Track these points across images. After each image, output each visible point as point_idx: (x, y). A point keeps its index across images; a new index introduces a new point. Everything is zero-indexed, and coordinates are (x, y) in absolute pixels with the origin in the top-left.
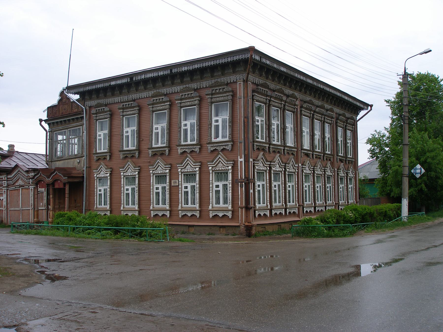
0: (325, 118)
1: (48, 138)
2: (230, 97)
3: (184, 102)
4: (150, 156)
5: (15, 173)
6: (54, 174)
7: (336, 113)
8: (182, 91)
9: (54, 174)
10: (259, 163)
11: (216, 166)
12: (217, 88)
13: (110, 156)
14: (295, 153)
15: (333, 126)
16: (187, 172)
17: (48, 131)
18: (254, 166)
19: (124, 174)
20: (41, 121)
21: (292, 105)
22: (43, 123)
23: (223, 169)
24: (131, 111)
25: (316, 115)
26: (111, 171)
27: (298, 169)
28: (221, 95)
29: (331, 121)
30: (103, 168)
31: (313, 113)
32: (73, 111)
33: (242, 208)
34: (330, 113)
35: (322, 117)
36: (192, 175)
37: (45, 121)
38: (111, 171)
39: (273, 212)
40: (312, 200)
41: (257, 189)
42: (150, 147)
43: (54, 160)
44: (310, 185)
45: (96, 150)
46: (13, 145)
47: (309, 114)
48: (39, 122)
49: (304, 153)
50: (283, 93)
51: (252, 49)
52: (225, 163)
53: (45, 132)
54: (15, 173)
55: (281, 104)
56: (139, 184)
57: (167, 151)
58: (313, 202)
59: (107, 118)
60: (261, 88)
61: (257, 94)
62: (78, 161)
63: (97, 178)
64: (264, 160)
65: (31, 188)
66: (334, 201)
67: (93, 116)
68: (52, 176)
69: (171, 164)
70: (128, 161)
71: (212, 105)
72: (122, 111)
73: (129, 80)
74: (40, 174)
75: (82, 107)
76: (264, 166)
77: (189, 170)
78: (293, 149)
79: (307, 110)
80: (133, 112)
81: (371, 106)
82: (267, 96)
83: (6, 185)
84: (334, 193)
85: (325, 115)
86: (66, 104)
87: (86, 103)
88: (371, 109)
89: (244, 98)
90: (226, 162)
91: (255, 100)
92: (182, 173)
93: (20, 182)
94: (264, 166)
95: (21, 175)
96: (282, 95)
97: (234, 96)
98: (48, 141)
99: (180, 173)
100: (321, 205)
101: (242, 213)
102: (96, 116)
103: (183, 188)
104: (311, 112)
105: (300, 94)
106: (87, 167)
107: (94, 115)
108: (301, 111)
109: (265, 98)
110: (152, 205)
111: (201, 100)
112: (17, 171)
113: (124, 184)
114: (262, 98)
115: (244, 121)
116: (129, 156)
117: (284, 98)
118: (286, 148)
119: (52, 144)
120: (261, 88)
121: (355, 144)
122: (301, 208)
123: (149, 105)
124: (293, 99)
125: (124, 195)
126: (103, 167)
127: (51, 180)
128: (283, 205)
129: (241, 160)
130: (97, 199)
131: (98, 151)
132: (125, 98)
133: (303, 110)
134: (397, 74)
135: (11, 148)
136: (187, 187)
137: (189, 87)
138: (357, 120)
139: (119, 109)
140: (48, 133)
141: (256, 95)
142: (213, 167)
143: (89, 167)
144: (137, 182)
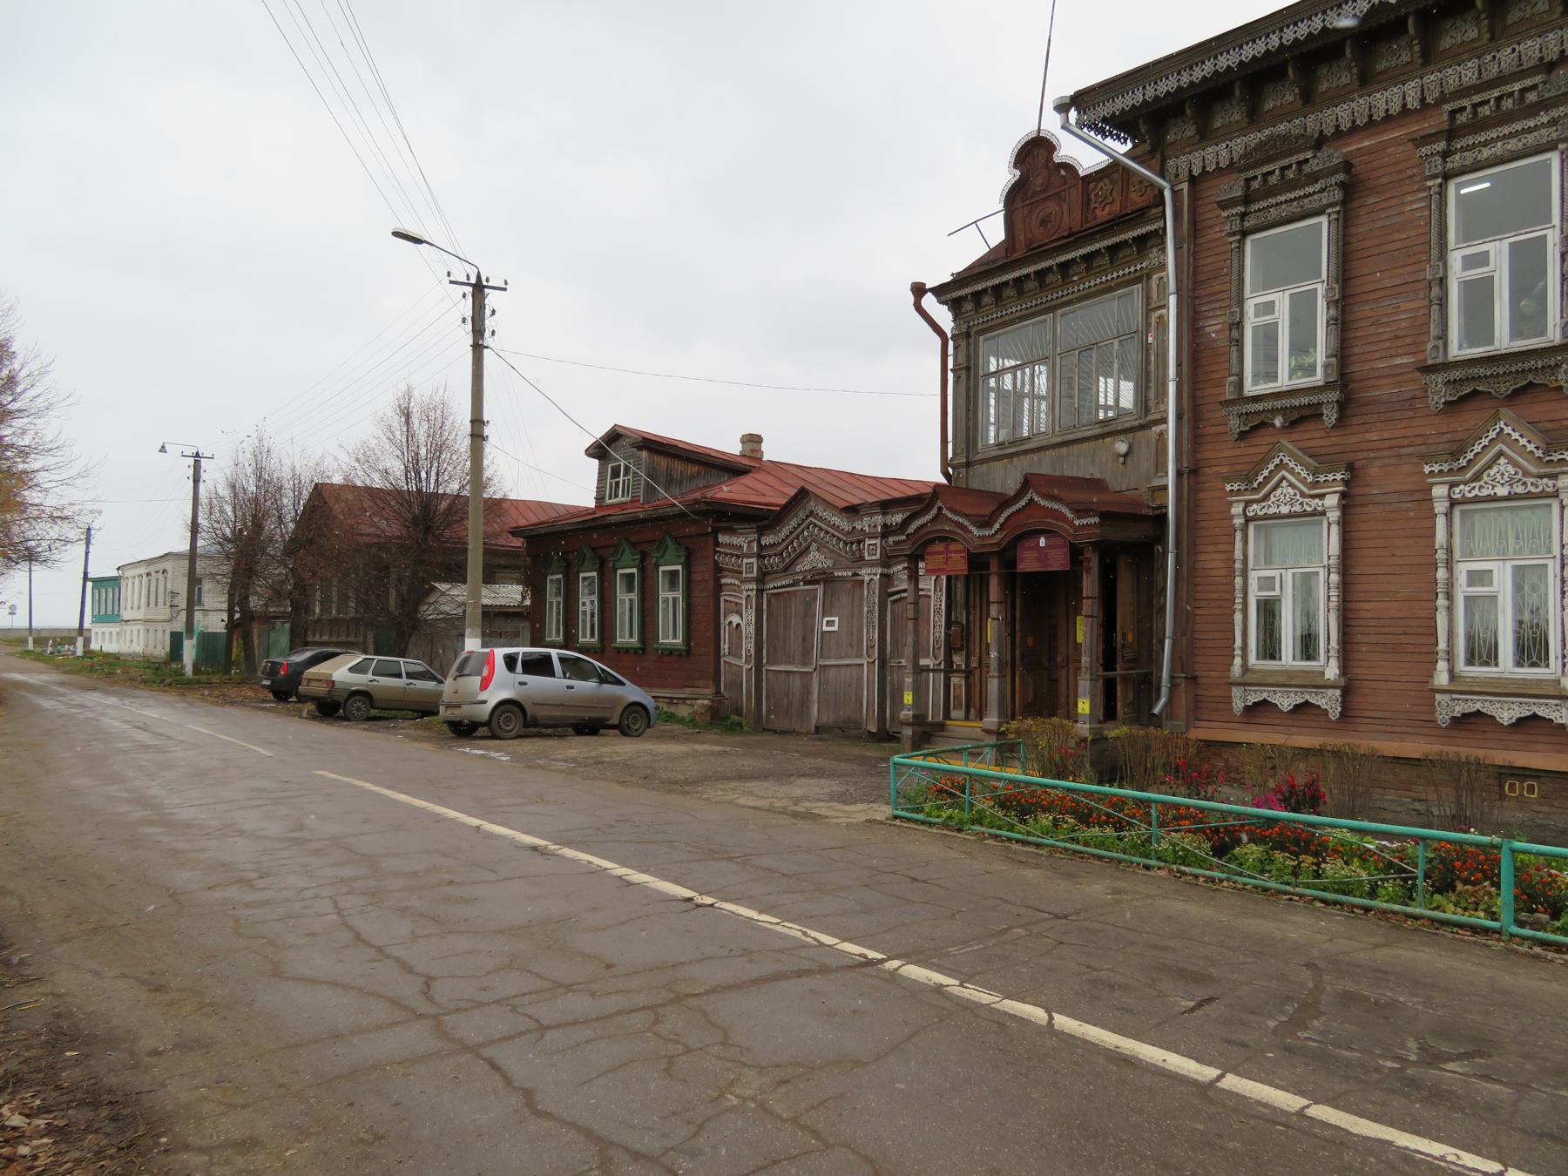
1: (950, 365)
5: (794, 523)
13: (1343, 406)
17: (949, 335)
19: (1457, 490)
20: (919, 290)
22: (929, 301)
24: (1511, 135)
26: (1346, 483)
30: (1292, 471)
32: (1095, 218)
37: (939, 291)
38: (1346, 483)
43: (979, 457)
45: (1240, 385)
46: (759, 436)
48: (911, 298)
53: (938, 341)
54: (794, 523)
62: (1122, 447)
65: (867, 579)
67: (1225, 214)
70: (1496, 418)
72: (1441, 146)
74: (934, 511)
75: (1152, 184)
80: (1530, 139)
83: (755, 574)
86: (1046, 199)
87: (1171, 163)
93: (815, 559)
95: (821, 529)
98: (950, 376)
102: (1243, 216)
103: (1462, 579)
106: (1179, 474)
107: (1234, 211)
112: (802, 515)
113: (1449, 550)
116: (1506, 388)
119: (968, 389)
125: (1450, 609)
126: (1292, 464)
127: (999, 536)
131: (1250, 389)
135: (750, 446)
140: (951, 344)
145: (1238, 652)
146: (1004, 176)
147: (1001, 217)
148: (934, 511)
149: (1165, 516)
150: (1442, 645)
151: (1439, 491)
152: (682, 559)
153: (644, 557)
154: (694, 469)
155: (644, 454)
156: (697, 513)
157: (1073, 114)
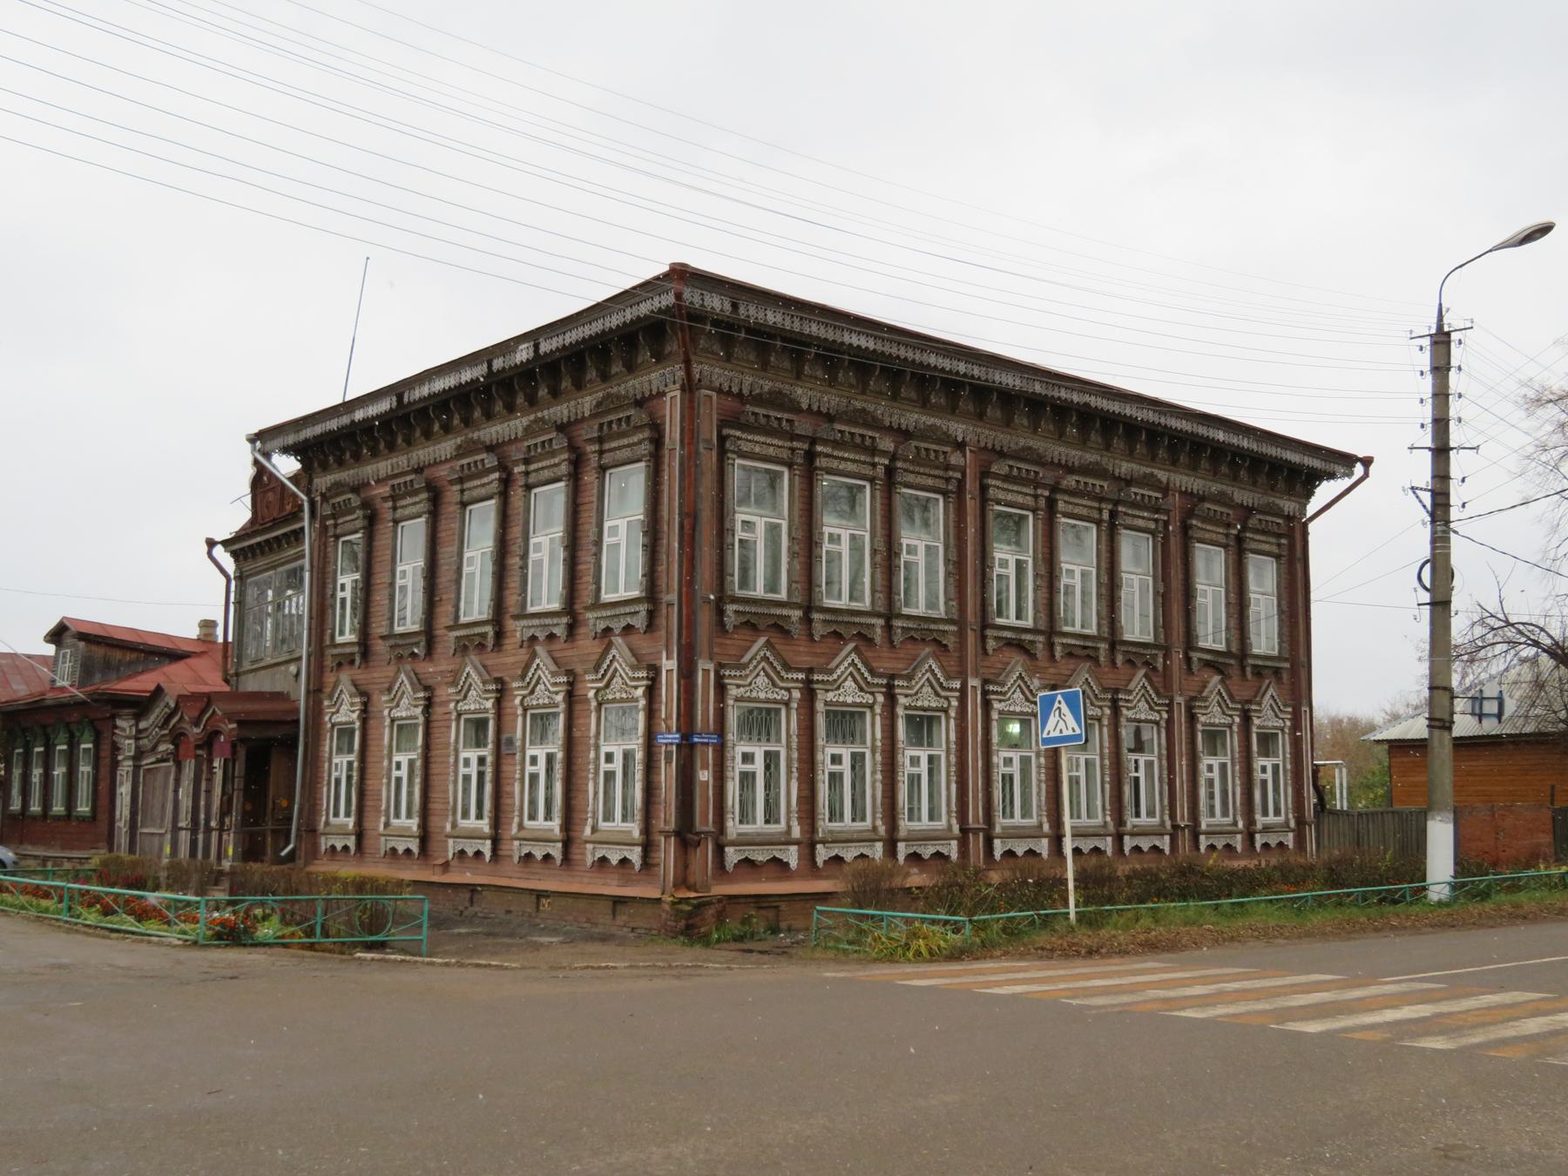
0: (1117, 512)
1: (232, 599)
2: (645, 448)
3: (536, 471)
4: (452, 651)
6: (207, 715)
7: (1181, 492)
8: (529, 432)
9: (207, 715)
10: (747, 676)
11: (608, 686)
12: (612, 417)
14: (950, 642)
15: (1166, 539)
16: (538, 706)
17: (232, 576)
18: (721, 689)
20: (211, 544)
21: (937, 468)
22: (219, 551)
23: (624, 696)
25: (1065, 502)
27: (963, 699)
28: (625, 441)
29: (1156, 521)
31: (1047, 493)
33: (667, 835)
34: (1141, 491)
35: (1100, 510)
36: (852, 714)
37: (225, 543)
39: (822, 853)
40: (1041, 810)
41: (737, 767)
42: (451, 623)
44: (1033, 755)
47: (1029, 498)
48: (205, 548)
49: (997, 638)
50: (875, 424)
51: (680, 273)
52: (627, 674)
53: (223, 581)
55: (874, 465)
56: (427, 747)
57: (491, 634)
58: (1045, 819)
59: (356, 532)
60: (757, 410)
61: (738, 433)
63: (333, 725)
64: (775, 664)
66: (1167, 818)
68: (205, 719)
69: (499, 680)
71: (604, 477)
72: (390, 504)
73: (395, 404)
76: (774, 685)
77: (541, 701)
78: (933, 627)
79: (1010, 482)
81: (1367, 462)
82: (793, 437)
84: (1166, 788)
85: (1117, 503)
88: (1366, 475)
89: (682, 447)
90: (630, 673)
91: (734, 452)
92: (525, 710)
94: (774, 685)
96: (870, 433)
97: (657, 441)
99: (520, 711)
100: (1032, 832)
101: (667, 852)
104: (1039, 491)
105: (975, 426)
108: (984, 489)
109: (788, 444)
110: (450, 818)
111: (577, 463)
114: (772, 445)
115: (681, 527)
117: (887, 444)
118: (898, 623)
120: (757, 410)
121: (1292, 603)
122: (977, 844)
123: (452, 482)
124: (934, 447)
128: (875, 828)
129: (669, 664)
130: (326, 794)
132: (401, 461)
133: (995, 486)
134: (1411, 332)
135: (206, 631)
136: (1011, 759)
137: (542, 419)
138: (1309, 514)
139: (385, 499)
140: (233, 584)
141: (735, 436)
142: (598, 690)
143: (315, 691)
144: (420, 741)
145: (324, 813)
146: (251, 471)
147: (249, 497)
148: (211, 711)
149: (297, 721)
150: (383, 807)
151: (386, 712)
152: (92, 739)
153: (72, 736)
154: (134, 656)
155: (82, 644)
156: (95, 701)
157: (258, 444)
